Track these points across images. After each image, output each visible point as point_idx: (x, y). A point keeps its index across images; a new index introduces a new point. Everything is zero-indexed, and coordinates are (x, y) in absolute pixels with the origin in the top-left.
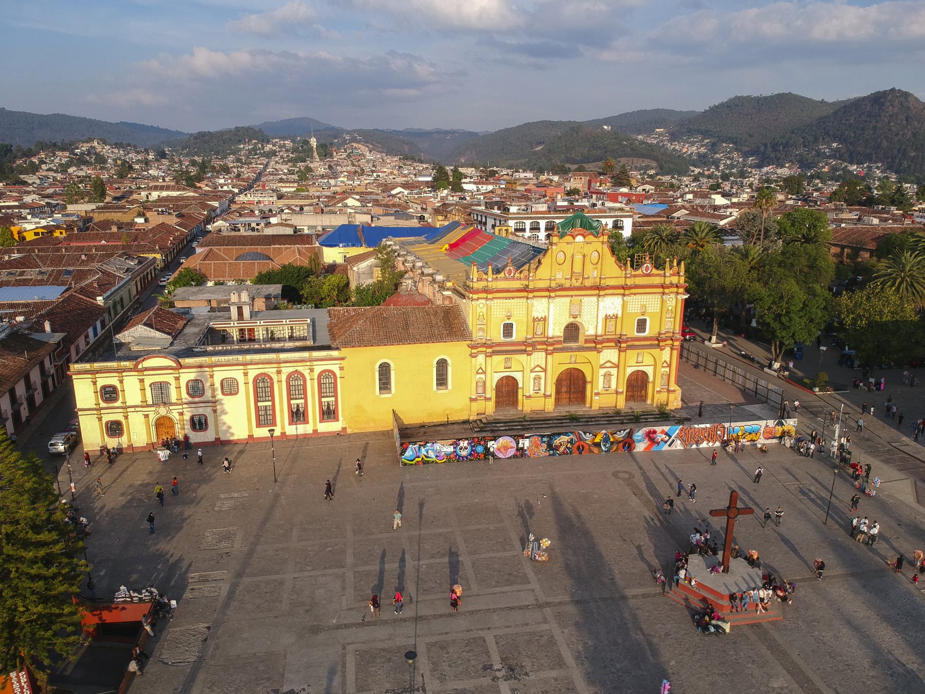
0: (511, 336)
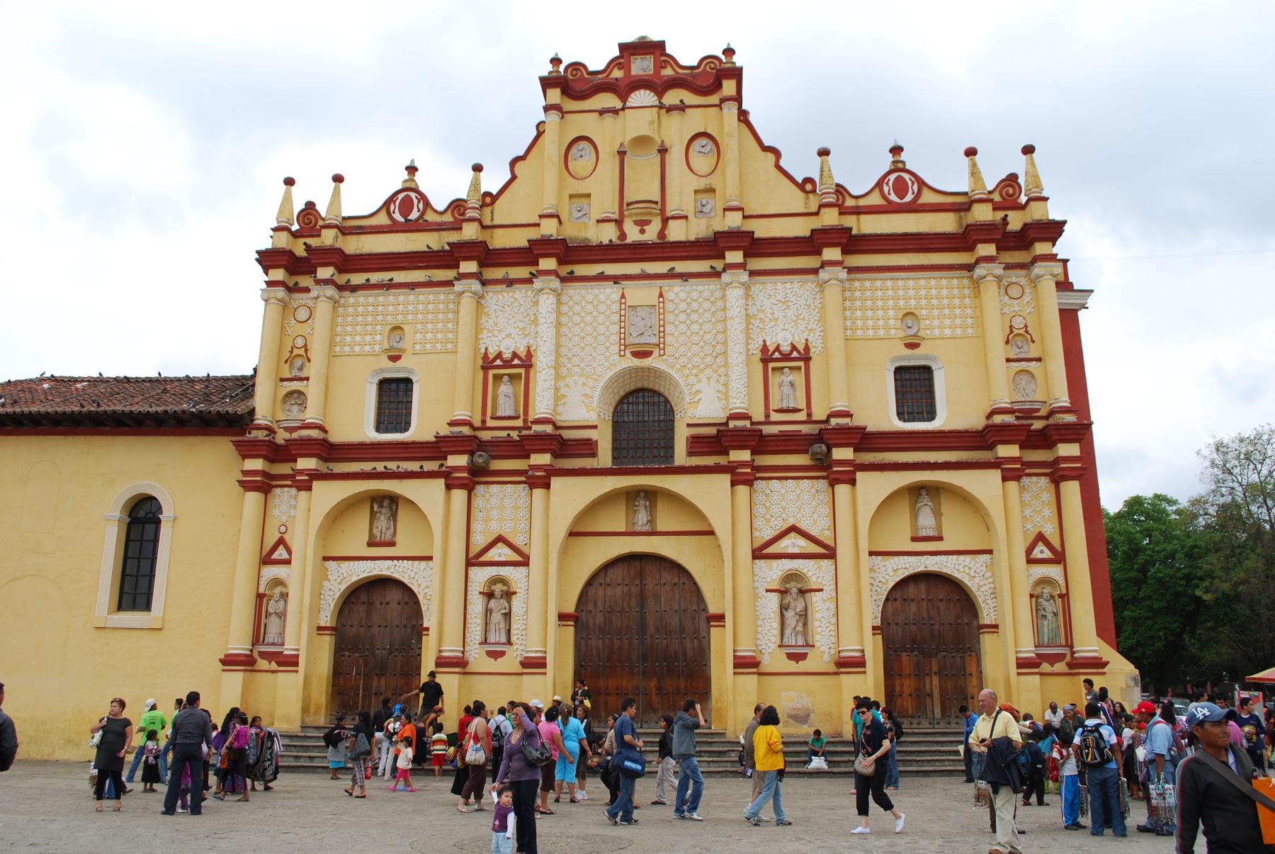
0: (405, 427)
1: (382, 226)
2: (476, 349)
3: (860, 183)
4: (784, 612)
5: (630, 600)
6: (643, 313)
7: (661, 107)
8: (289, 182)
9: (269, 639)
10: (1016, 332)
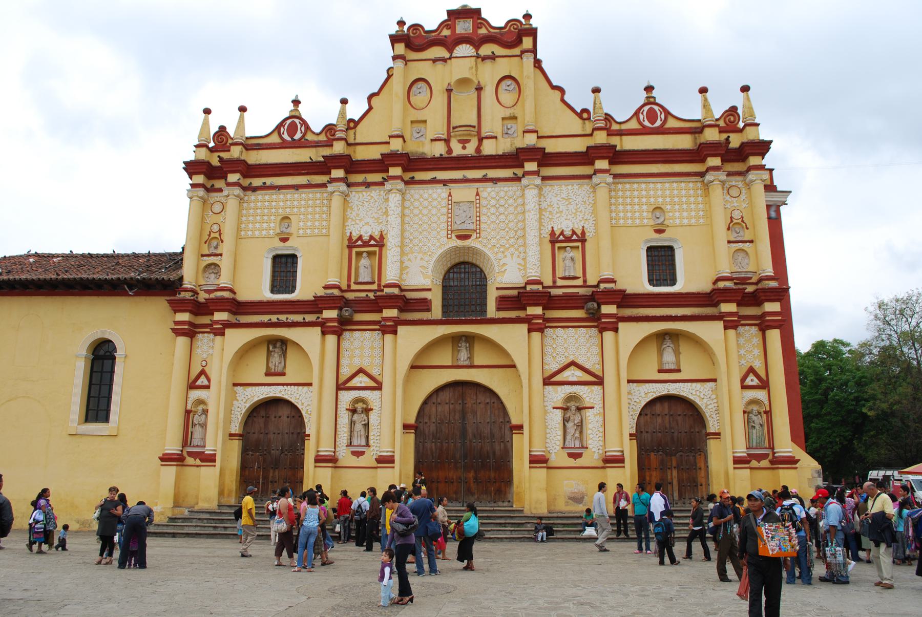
0: (292, 289)
1: (274, 144)
2: (344, 233)
3: (622, 114)
4: (566, 423)
5: (455, 415)
6: (464, 207)
7: (478, 56)
8: (207, 111)
9: (195, 442)
10: (735, 221)
